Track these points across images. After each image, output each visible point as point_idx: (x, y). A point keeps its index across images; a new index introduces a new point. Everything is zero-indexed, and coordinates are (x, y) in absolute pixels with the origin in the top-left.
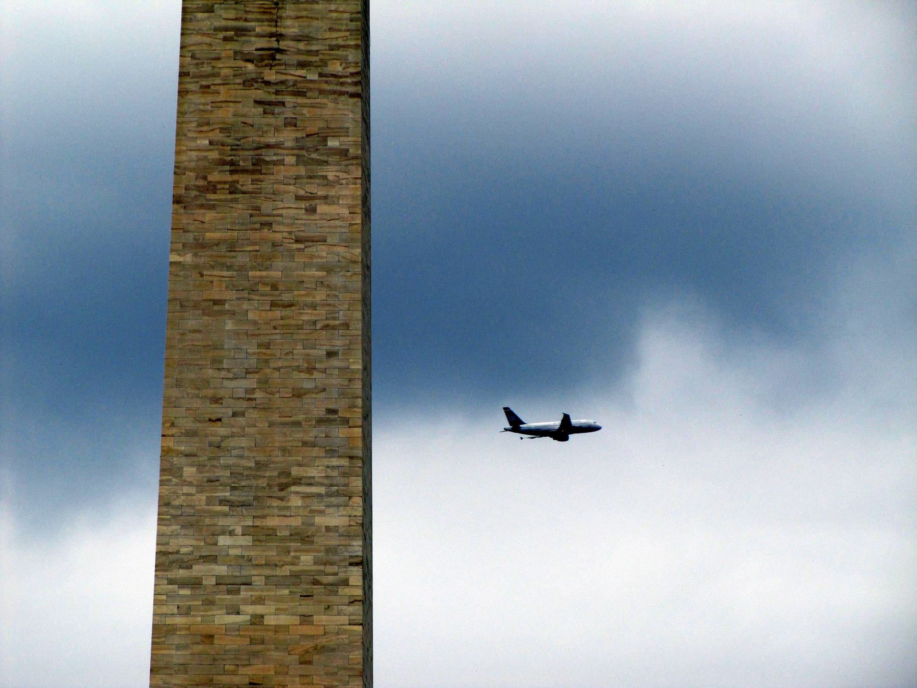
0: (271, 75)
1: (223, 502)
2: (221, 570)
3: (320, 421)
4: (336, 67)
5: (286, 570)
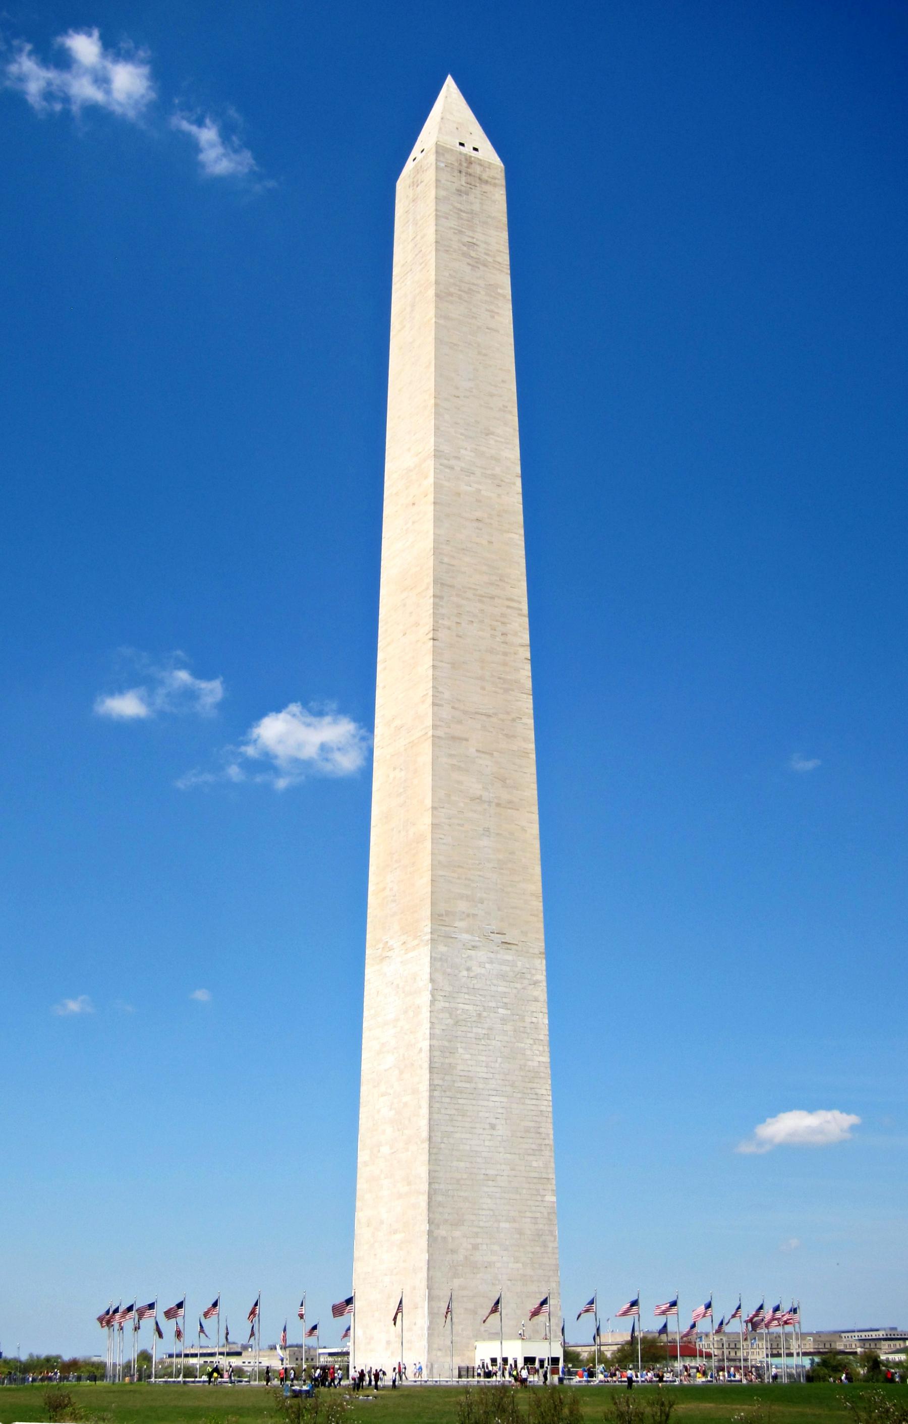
0: (473, 254)
1: (462, 434)
2: (463, 465)
4: (499, 259)
5: (489, 472)
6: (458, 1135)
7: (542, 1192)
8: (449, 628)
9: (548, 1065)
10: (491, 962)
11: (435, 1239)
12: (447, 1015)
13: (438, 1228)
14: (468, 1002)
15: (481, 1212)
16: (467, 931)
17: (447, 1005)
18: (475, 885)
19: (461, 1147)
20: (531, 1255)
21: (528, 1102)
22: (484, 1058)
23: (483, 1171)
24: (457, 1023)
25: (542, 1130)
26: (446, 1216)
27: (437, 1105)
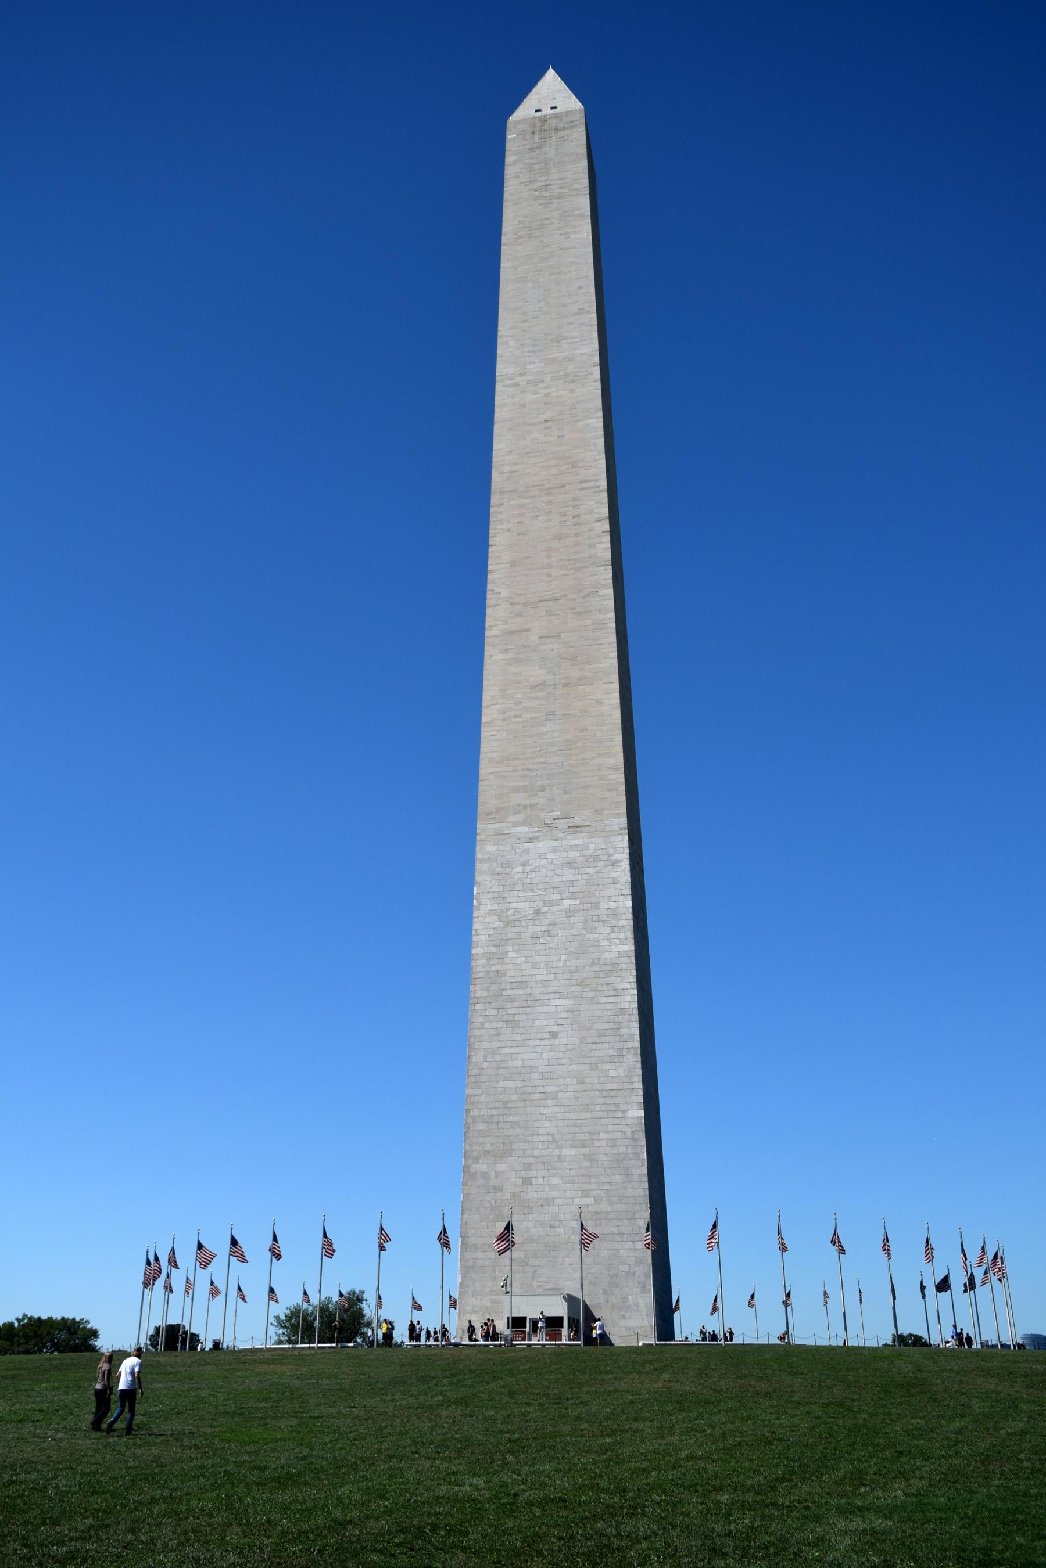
0: (544, 194)
2: (529, 378)
3: (575, 314)
4: (578, 186)
5: (561, 373)
6: (507, 1050)
7: (623, 1107)
8: (509, 530)
9: (633, 954)
10: (555, 850)
11: (473, 1176)
12: (496, 918)
13: (477, 1163)
14: (523, 899)
15: (535, 1138)
16: (523, 824)
17: (496, 907)
18: (534, 774)
19: (510, 1064)
20: (607, 1187)
21: (603, 1000)
22: (543, 959)
23: (541, 1089)
24: (507, 926)
25: (622, 1031)
26: (488, 1147)
27: (480, 1019)
